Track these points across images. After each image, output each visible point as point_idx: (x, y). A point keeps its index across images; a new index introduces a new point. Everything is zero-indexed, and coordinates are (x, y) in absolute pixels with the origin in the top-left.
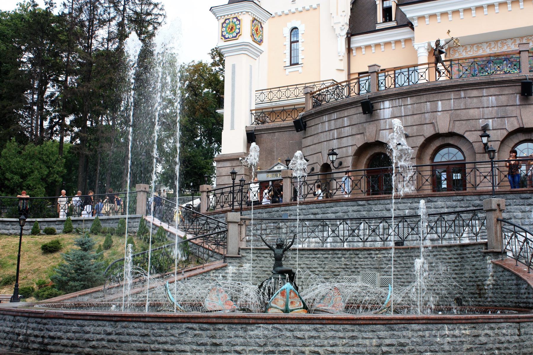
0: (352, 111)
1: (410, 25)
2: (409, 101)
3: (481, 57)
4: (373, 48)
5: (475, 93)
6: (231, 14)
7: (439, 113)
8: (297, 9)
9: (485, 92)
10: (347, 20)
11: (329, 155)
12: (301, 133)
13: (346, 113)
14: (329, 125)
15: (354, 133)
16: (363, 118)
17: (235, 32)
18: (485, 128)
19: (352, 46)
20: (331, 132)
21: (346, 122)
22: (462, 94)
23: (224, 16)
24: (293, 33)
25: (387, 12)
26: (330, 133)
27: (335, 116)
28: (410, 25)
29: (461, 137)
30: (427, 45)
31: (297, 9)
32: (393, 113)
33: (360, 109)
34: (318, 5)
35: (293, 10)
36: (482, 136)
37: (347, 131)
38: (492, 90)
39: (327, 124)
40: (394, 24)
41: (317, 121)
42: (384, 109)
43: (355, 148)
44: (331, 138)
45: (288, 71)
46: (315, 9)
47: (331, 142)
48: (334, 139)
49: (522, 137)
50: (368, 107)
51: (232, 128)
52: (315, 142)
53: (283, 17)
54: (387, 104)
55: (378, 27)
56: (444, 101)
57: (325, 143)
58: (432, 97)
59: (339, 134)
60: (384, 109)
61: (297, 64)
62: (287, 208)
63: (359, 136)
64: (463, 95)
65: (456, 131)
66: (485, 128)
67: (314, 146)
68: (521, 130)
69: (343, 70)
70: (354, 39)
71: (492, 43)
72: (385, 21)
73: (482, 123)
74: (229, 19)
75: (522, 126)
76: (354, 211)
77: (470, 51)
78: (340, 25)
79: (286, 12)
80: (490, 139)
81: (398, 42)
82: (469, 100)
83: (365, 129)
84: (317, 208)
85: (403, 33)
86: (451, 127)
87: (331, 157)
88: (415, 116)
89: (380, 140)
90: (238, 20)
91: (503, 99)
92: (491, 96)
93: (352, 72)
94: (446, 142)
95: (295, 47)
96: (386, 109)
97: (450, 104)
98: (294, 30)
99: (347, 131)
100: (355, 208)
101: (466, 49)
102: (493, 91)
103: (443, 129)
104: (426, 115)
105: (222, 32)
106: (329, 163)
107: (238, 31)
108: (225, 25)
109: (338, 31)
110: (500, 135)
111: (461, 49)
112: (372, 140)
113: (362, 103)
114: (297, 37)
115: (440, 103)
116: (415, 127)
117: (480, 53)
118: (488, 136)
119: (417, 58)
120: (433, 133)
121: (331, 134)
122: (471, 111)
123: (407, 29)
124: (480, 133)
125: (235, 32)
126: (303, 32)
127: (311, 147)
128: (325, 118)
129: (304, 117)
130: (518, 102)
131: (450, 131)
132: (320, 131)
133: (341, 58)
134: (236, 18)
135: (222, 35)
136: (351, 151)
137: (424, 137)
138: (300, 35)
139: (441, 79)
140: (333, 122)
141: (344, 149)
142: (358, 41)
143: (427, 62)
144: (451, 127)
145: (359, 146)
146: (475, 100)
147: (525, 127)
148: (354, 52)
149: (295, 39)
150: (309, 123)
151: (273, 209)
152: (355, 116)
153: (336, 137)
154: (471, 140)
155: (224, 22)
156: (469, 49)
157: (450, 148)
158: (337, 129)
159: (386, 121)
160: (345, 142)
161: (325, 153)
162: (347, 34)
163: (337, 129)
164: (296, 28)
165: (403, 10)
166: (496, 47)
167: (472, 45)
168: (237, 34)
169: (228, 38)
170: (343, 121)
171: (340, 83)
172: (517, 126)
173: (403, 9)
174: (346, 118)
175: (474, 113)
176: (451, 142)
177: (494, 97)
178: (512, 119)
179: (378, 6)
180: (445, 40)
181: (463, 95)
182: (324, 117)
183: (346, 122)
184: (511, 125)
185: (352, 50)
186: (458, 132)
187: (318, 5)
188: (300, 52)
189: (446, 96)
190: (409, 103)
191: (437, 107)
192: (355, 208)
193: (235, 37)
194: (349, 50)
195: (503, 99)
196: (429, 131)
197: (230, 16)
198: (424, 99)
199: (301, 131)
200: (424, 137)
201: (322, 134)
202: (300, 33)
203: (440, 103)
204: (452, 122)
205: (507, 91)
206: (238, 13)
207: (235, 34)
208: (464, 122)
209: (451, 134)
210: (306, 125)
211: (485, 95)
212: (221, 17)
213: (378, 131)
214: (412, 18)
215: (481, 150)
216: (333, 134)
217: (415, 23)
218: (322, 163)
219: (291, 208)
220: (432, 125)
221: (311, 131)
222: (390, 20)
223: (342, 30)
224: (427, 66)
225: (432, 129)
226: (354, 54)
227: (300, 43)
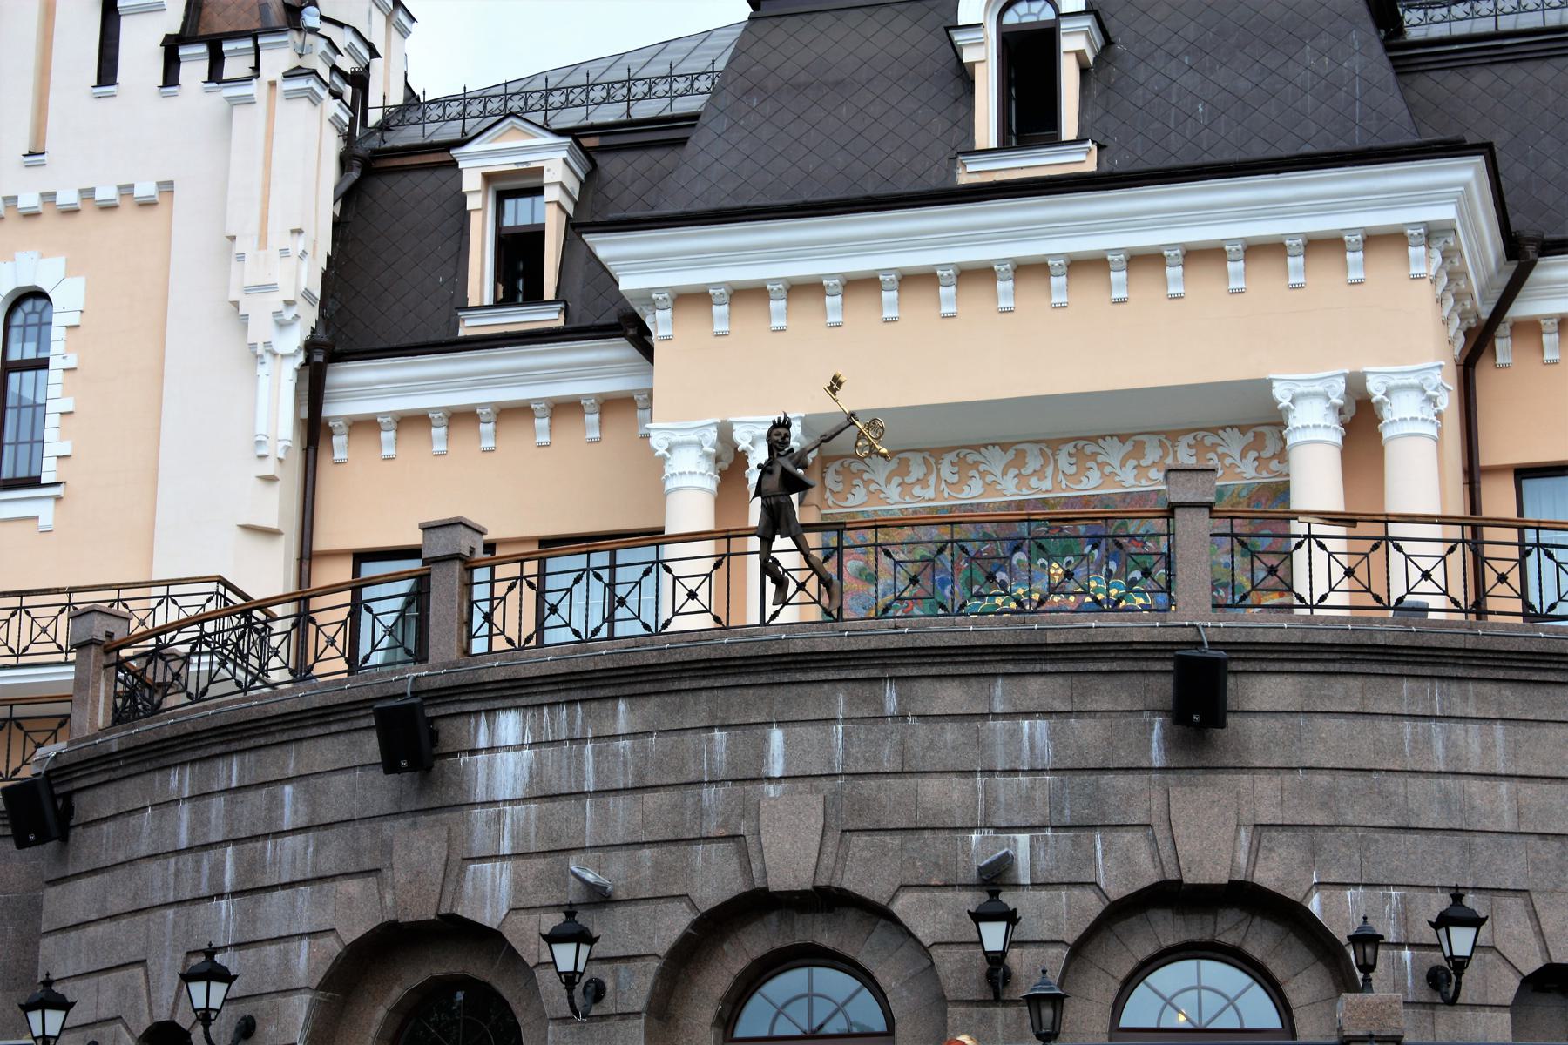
0: (323, 752)
1: (632, 330)
2: (624, 716)
4: (438, 432)
5: (951, 696)
7: (771, 790)
8: (48, 197)
9: (1000, 695)
10: (310, 276)
11: (188, 977)
12: (40, 857)
13: (291, 761)
14: (199, 822)
15: (328, 867)
16: (380, 790)
18: (995, 877)
19: (333, 410)
20: (207, 859)
21: (290, 806)
22: (891, 699)
24: (18, 318)
25: (519, 257)
26: (198, 863)
27: (232, 772)
28: (632, 330)
29: (878, 914)
30: (712, 435)
31: (48, 197)
32: (535, 773)
33: (370, 746)
34: (167, 187)
35: (29, 200)
36: (978, 917)
37: (291, 856)
38: (1035, 685)
39: (184, 812)
40: (549, 317)
41: (131, 792)
43: (332, 947)
44: (204, 890)
46: (147, 204)
47: (201, 909)
48: (221, 896)
49: (1169, 929)
50: (413, 736)
52: (116, 904)
54: (509, 726)
55: (469, 326)
56: (798, 730)
57: (170, 912)
58: (743, 703)
59: (247, 867)
60: (492, 749)
61: (34, 482)
63: (353, 887)
64: (891, 705)
65: (852, 881)
66: (995, 877)
68: (1170, 896)
69: (272, 533)
70: (345, 376)
71: (1032, 450)
72: (507, 299)
73: (979, 847)
75: (1172, 875)
77: (922, 482)
78: (275, 301)
80: (1020, 932)
82: (923, 730)
83: (387, 848)
85: (594, 368)
86: (828, 860)
87: (198, 990)
88: (651, 799)
89: (465, 911)
91: (1088, 735)
92: (1028, 715)
93: (321, 543)
94: (800, 937)
95: (28, 394)
96: (504, 754)
97: (827, 745)
98: (28, 306)
99: (291, 856)
102: (1037, 690)
104: (708, 794)
106: (185, 1020)
109: (261, 330)
110: (1068, 914)
111: (881, 470)
112: (422, 910)
113: (381, 715)
114: (43, 342)
115: (777, 736)
116: (647, 852)
117: (973, 493)
118: (1010, 917)
119: (660, 497)
120: (737, 887)
122: (932, 788)
123: (617, 350)
124: (971, 900)
126: (74, 319)
127: (91, 929)
128: (180, 781)
129: (60, 771)
130: (1157, 757)
131: (823, 881)
132: (144, 850)
133: (269, 468)
136: (307, 963)
137: (693, 905)
138: (57, 333)
139: (788, 615)
140: (218, 803)
141: (272, 949)
142: (365, 388)
143: (707, 524)
144: (828, 860)
145: (349, 938)
146: (951, 732)
147: (1189, 879)
148: (337, 441)
149: (30, 353)
150: (86, 806)
152: (339, 781)
153: (229, 881)
154: (924, 931)
156: (917, 471)
157: (817, 971)
158: (236, 841)
159: (499, 817)
160: (276, 913)
161: (168, 969)
162: (310, 346)
163: (236, 841)
164: (38, 294)
165: (602, 252)
166: (1049, 470)
167: (933, 454)
170: (276, 803)
171: (263, 605)
172: (1148, 874)
173: (606, 247)
174: (288, 789)
175: (941, 795)
176: (827, 940)
177: (1041, 725)
178: (1127, 836)
179: (475, 221)
181: (891, 705)
182: (174, 777)
183: (290, 806)
184: (1123, 867)
185: (330, 433)
186: (861, 890)
187: (167, 187)
188: (52, 420)
189: (809, 702)
190: (622, 726)
191: (762, 754)
194: (314, 431)
195: (1088, 735)
196: (714, 879)
198: (698, 709)
199: (42, 839)
200: (693, 905)
201: (155, 866)
202: (57, 320)
203: (777, 736)
204: (833, 836)
205: (1106, 695)
208: (893, 841)
209: (827, 900)
210: (69, 810)
211: (999, 708)
213: (458, 862)
214: (647, 297)
215: (975, 986)
216: (218, 869)
217: (660, 323)
218: (146, 1023)
220: (730, 846)
221: (94, 845)
222: (534, 296)
223: (282, 325)
224: (708, 547)
225: (734, 865)
226: (339, 455)
227: (54, 374)
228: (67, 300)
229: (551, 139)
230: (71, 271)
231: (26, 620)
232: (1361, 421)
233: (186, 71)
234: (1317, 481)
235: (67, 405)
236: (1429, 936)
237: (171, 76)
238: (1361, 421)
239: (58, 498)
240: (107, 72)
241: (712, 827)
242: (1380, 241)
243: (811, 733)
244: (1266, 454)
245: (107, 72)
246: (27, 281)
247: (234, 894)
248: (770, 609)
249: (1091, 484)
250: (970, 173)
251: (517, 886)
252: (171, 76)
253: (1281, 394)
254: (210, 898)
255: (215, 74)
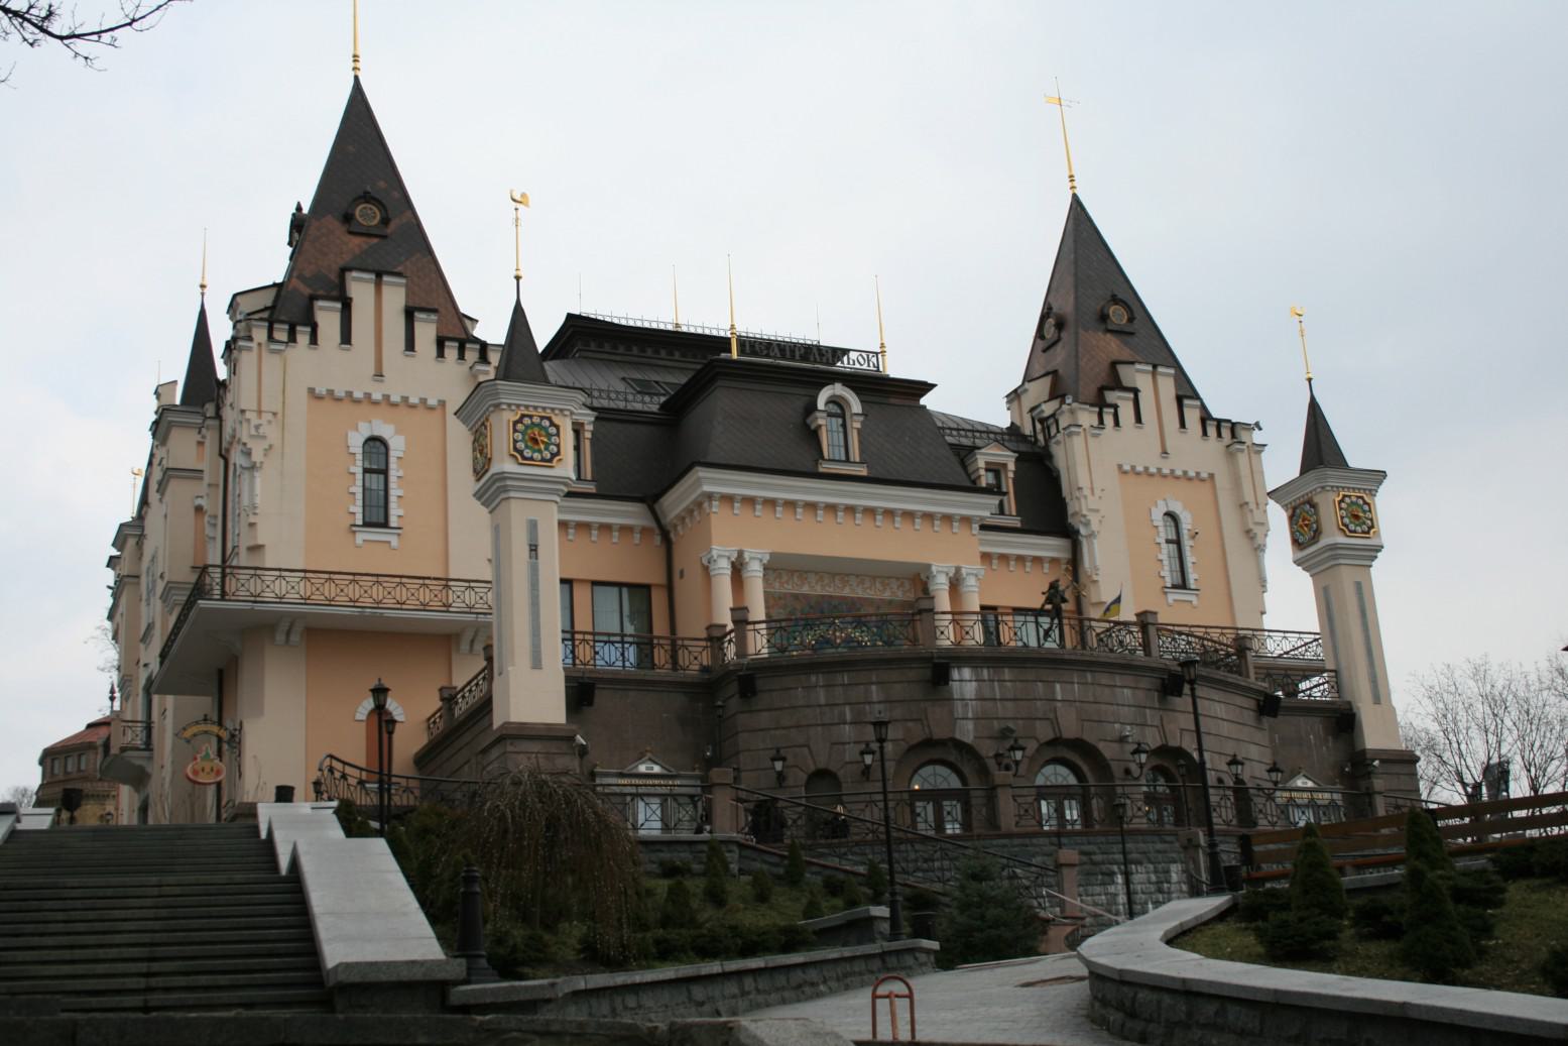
2: (1007, 674)
3: (806, 597)
5: (1105, 679)
6: (536, 408)
7: (1059, 704)
9: (1118, 680)
17: (527, 447)
20: (836, 711)
23: (518, 406)
30: (736, 555)
31: (387, 397)
32: (979, 690)
42: (961, 681)
44: (836, 721)
45: (360, 537)
48: (845, 723)
51: (537, 664)
53: (328, 404)
54: (967, 673)
57: (819, 728)
61: (385, 525)
62: (1027, 841)
63: (910, 724)
67: (783, 732)
74: (531, 417)
76: (1158, 852)
79: (358, 395)
81: (606, 528)
84: (1089, 843)
89: (958, 736)
90: (552, 424)
96: (965, 683)
100: (1159, 846)
101: (780, 576)
102: (1129, 680)
103: (1070, 730)
104: (1039, 703)
105: (515, 441)
107: (555, 449)
108: (520, 427)
112: (939, 733)
115: (1058, 686)
117: (805, 590)
120: (1051, 736)
121: (836, 712)
125: (527, 447)
126: (401, 455)
127: (773, 732)
134: (549, 419)
135: (515, 449)
137: (1038, 740)
139: (1047, 645)
146: (1107, 691)
150: (760, 684)
151: (995, 842)
153: (848, 717)
155: (520, 421)
159: (967, 705)
163: (850, 704)
166: (791, 583)
167: (792, 572)
168: (554, 455)
169: (532, 459)
174: (874, 687)
180: (771, 554)
182: (813, 678)
192: (1159, 846)
193: (524, 458)
197: (531, 412)
200: (1038, 740)
203: (1058, 686)
206: (553, 409)
207: (529, 455)
211: (1118, 684)
212: (509, 405)
213: (953, 721)
214: (710, 496)
218: (812, 768)
219: (1035, 841)
228: (397, 445)
229: (589, 412)
230: (398, 432)
231: (284, 582)
232: (955, 584)
233: (447, 352)
234: (943, 602)
235: (400, 493)
236: (1225, 768)
237: (441, 354)
238: (955, 584)
239: (399, 535)
240: (410, 345)
241: (1040, 715)
242: (966, 520)
243: (1068, 686)
244: (865, 586)
245: (410, 345)
246: (376, 433)
247: (851, 723)
248: (1042, 641)
249: (846, 592)
250: (824, 468)
251: (976, 728)
252: (441, 354)
253: (934, 569)
254: (839, 724)
255: (461, 356)
